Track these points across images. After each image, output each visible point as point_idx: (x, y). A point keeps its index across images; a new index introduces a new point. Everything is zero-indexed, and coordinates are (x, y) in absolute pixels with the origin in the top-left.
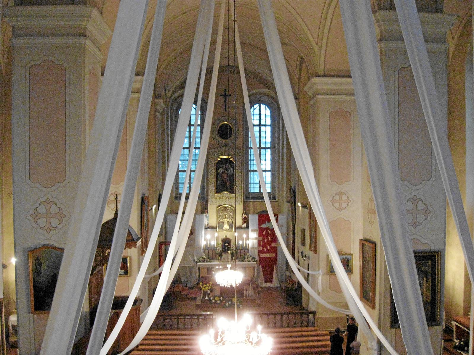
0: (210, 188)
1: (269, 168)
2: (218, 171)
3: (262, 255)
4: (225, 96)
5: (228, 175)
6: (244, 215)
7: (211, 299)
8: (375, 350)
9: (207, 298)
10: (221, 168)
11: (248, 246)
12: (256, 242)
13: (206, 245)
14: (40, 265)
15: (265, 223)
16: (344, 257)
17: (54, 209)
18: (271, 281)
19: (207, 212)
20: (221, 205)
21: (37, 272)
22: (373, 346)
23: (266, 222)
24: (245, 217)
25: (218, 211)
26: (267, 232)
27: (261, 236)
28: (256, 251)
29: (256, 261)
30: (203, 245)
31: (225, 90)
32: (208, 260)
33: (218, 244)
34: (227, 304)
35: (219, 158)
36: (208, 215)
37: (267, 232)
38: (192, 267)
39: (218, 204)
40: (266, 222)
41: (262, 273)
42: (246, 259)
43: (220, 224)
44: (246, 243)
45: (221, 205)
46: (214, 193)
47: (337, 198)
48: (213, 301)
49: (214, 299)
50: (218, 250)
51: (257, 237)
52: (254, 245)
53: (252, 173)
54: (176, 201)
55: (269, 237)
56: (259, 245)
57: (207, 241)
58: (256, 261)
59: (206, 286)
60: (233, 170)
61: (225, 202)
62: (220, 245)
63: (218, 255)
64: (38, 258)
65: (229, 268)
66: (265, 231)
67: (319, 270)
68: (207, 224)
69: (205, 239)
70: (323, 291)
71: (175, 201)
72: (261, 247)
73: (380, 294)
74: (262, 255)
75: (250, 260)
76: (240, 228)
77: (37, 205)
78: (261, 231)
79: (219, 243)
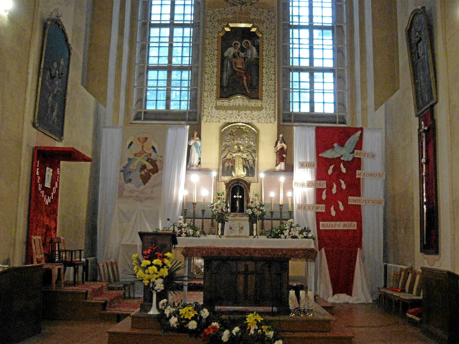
0: (207, 87)
1: (329, 64)
2: (226, 54)
3: (325, 225)
5: (246, 60)
6: (279, 145)
7: (167, 312)
9: (153, 312)
10: (232, 46)
11: (290, 203)
12: (309, 192)
13: (191, 195)
15: (333, 147)
18: (349, 292)
19: (199, 136)
20: (229, 124)
23: (335, 145)
24: (282, 149)
25: (222, 136)
26: (337, 169)
27: (323, 180)
28: (311, 215)
29: (314, 239)
30: (180, 199)
32: (191, 231)
33: (218, 195)
34: (225, 336)
35: (227, 26)
37: (337, 169)
39: (223, 122)
40: (335, 145)
42: (286, 233)
43: (227, 164)
44: (285, 198)
45: (229, 124)
48: (173, 321)
49: (177, 313)
50: (217, 208)
51: (314, 179)
52: (305, 199)
53: (296, 75)
54: (137, 122)
55: (342, 182)
56: (319, 200)
58: (312, 238)
59: (152, 265)
60: (258, 51)
61: (239, 118)
62: (224, 196)
66: (332, 167)
69: (188, 185)
71: (134, 122)
72: (324, 205)
74: (325, 225)
75: (297, 234)
76: (271, 172)
79: (221, 192)
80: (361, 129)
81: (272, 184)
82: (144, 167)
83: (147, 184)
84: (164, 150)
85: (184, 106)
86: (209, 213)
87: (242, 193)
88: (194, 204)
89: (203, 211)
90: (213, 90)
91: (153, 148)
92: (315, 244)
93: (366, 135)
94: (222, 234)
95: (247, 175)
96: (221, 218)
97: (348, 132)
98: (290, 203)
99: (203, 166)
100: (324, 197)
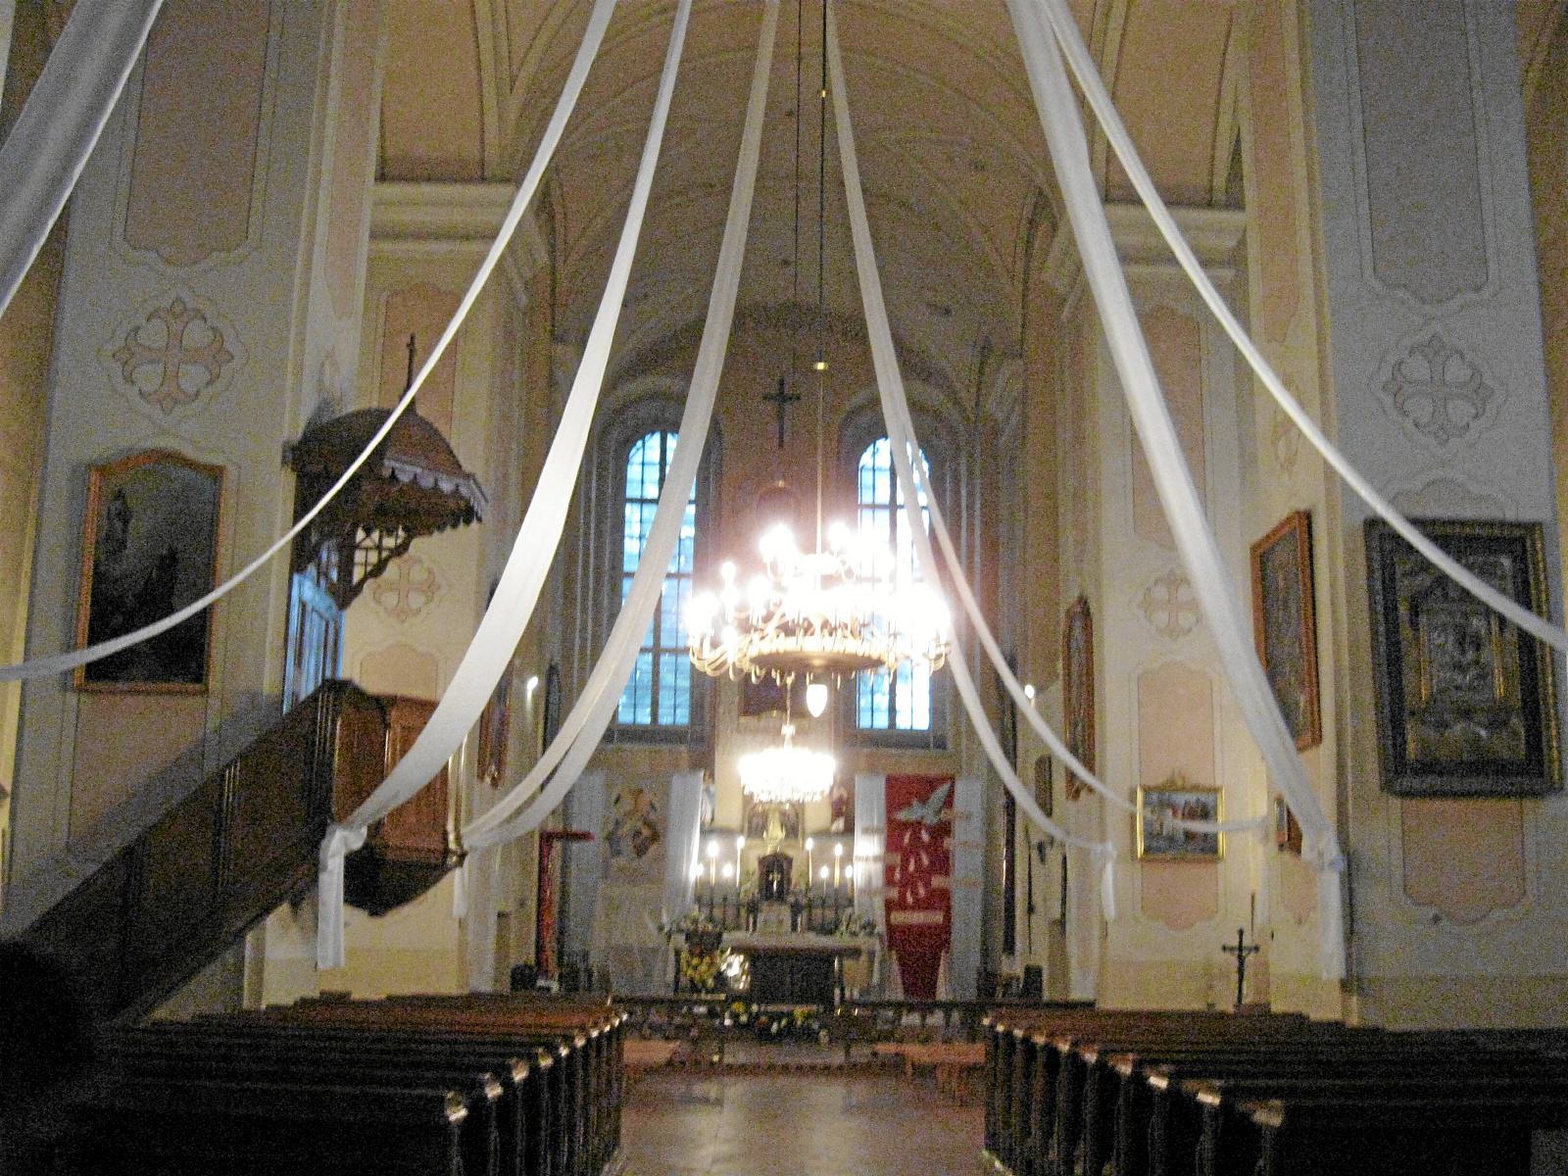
3: (899, 918)
4: (782, 397)
8: (1332, 864)
11: (849, 885)
12: (877, 869)
14: (124, 517)
16: (1192, 798)
17: (196, 335)
21: (113, 543)
22: (1321, 854)
23: (915, 802)
26: (916, 837)
31: (782, 383)
33: (746, 874)
34: (775, 1027)
36: (712, 789)
37: (916, 837)
38: (655, 950)
40: (915, 802)
41: (896, 967)
43: (755, 821)
46: (735, 713)
47: (1161, 592)
52: (869, 881)
56: (889, 881)
57: (707, 866)
62: (756, 877)
63: (743, 912)
64: (120, 495)
65: (788, 737)
67: (1103, 840)
68: (708, 817)
69: (702, 858)
70: (1120, 918)
73: (1337, 672)
76: (823, 835)
77: (132, 393)
78: (895, 834)
79: (751, 870)
80: (952, 779)
81: (822, 856)
82: (638, 833)
83: (644, 858)
84: (666, 805)
85: (683, 717)
86: (732, 899)
87: (781, 872)
88: (712, 889)
89: (725, 899)
90: (733, 703)
91: (652, 806)
92: (881, 942)
93: (959, 788)
94: (754, 930)
95: (787, 836)
96: (753, 908)
97: (931, 784)
98: (849, 885)
99: (720, 822)
100: (897, 876)
